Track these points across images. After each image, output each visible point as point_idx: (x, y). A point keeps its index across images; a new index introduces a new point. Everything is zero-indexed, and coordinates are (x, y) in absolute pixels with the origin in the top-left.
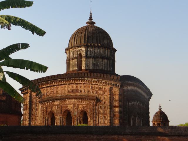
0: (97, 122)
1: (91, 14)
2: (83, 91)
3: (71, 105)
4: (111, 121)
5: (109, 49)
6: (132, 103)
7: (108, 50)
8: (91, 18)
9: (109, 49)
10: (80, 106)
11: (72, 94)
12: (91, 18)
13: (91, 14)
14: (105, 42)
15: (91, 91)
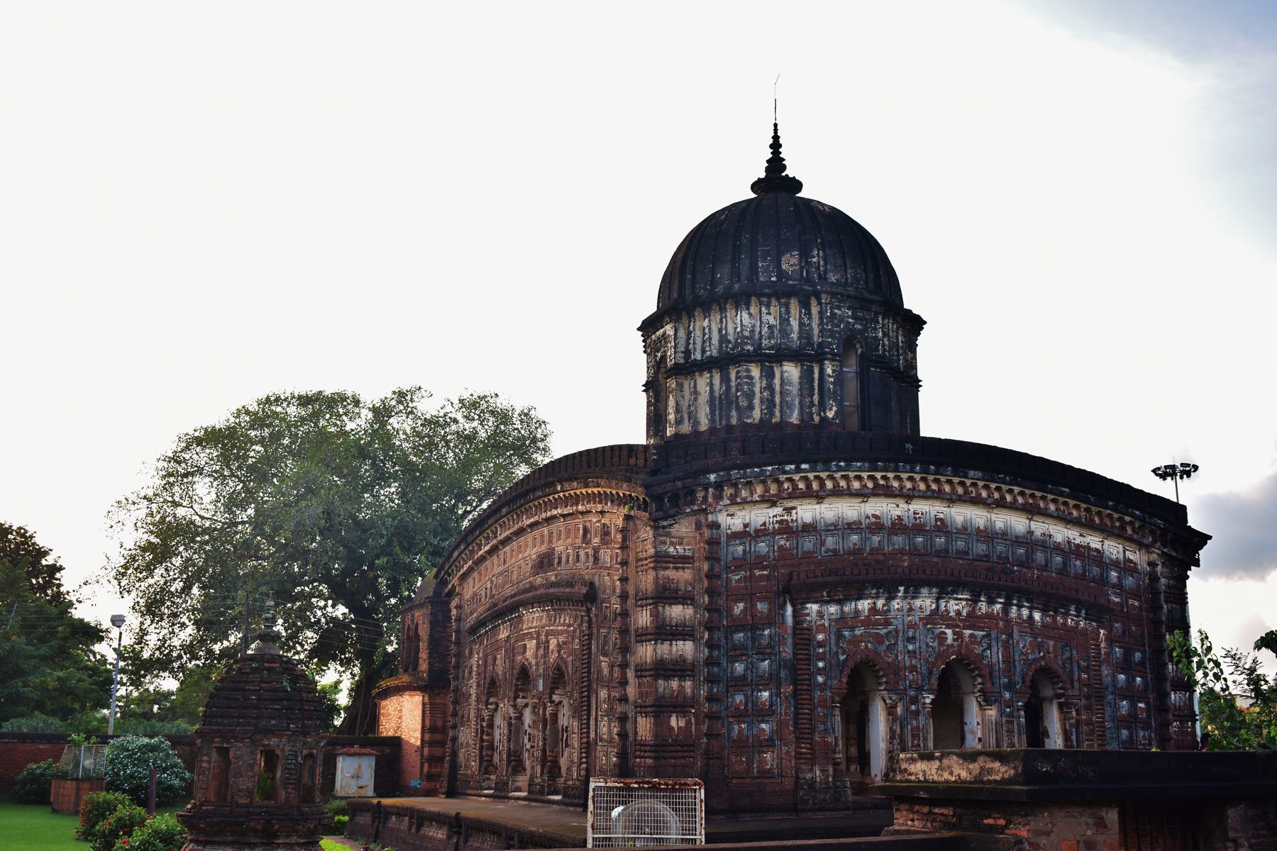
0: (592, 735)
1: (776, 137)
2: (564, 559)
3: (532, 638)
4: (629, 726)
5: (814, 302)
6: (864, 605)
7: (806, 305)
8: (776, 163)
9: (814, 302)
10: (553, 643)
11: (539, 580)
12: (776, 163)
13: (776, 137)
14: (784, 267)
15: (582, 553)
